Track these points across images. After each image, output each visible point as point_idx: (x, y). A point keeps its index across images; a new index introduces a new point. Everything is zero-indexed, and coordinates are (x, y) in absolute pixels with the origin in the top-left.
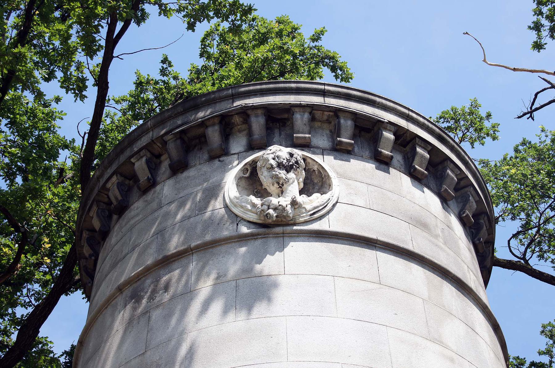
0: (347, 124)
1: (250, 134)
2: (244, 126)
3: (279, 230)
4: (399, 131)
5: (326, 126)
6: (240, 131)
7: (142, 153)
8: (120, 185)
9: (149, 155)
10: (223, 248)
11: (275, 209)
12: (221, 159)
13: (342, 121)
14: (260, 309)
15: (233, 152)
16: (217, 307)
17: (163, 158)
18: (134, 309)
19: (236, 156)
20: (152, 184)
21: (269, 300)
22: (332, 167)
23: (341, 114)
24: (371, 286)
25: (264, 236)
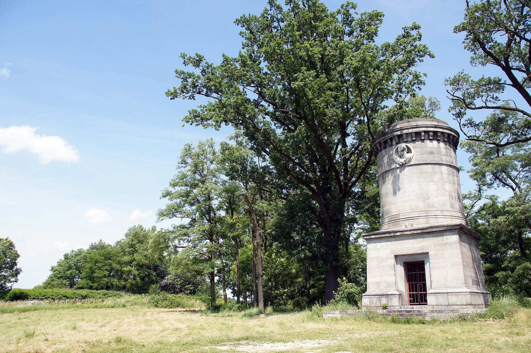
0: (414, 135)
4: (425, 132)
20: (381, 150)
22: (412, 146)
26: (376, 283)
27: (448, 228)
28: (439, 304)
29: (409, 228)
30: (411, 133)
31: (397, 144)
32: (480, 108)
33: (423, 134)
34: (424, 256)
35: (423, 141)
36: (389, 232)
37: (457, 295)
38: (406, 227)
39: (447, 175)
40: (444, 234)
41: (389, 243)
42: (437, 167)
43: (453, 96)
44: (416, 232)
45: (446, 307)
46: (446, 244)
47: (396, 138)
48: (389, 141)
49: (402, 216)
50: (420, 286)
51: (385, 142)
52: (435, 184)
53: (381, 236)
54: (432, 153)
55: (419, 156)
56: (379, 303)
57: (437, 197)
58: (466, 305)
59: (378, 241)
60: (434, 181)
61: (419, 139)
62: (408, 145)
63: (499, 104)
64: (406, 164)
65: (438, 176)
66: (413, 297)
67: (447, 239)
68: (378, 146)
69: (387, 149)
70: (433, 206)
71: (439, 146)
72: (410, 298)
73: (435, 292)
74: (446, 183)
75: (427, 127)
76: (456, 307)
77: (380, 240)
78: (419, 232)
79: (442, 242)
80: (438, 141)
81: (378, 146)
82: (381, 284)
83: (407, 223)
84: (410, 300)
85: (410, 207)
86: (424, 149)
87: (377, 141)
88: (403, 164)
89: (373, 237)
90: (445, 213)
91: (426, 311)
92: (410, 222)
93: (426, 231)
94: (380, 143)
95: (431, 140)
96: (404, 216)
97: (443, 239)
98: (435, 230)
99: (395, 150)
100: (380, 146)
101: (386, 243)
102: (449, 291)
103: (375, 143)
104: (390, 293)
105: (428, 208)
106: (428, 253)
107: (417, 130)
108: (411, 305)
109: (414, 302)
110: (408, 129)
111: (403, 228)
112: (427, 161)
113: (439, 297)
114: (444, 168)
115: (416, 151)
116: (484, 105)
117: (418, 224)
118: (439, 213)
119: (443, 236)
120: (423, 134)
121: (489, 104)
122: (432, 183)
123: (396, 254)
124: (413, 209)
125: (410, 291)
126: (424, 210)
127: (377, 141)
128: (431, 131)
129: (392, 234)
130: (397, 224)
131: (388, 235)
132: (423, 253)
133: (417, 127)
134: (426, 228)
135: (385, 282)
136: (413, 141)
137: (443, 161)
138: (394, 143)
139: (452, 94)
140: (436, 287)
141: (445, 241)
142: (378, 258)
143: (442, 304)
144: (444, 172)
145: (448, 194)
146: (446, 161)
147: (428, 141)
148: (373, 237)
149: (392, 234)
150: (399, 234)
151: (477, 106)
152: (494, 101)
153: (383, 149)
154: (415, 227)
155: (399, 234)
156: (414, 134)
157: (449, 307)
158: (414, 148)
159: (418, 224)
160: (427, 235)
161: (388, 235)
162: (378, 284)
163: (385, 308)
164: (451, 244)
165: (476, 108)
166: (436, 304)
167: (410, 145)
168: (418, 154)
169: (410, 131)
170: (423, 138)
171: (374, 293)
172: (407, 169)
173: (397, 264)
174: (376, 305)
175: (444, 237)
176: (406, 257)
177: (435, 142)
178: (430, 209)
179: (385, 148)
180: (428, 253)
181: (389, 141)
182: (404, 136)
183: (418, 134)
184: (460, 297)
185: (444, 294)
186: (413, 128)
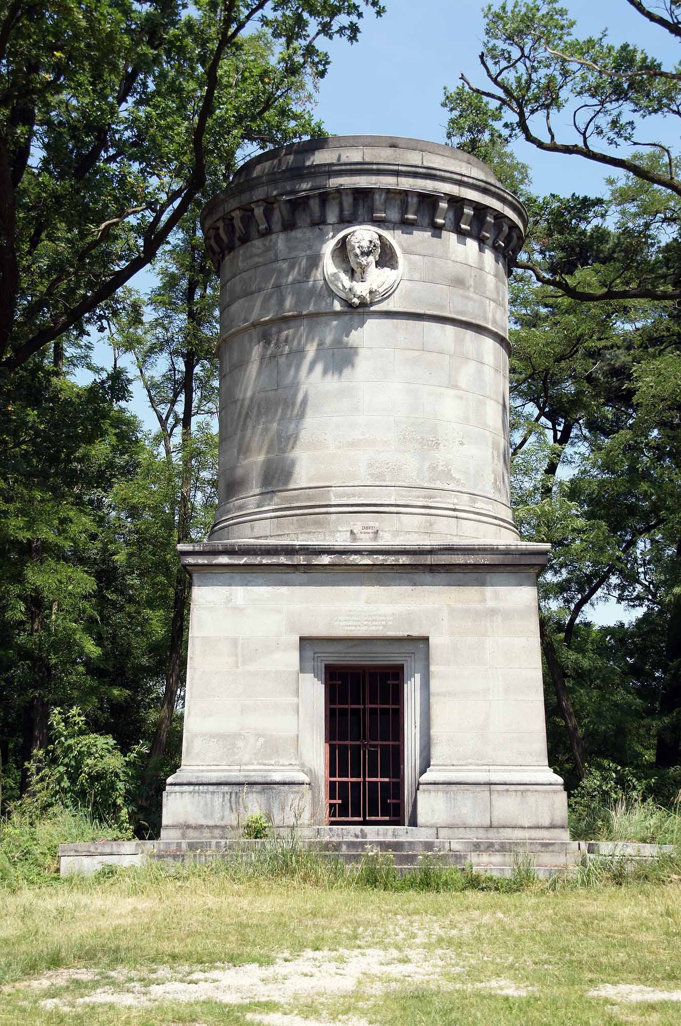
0: (413, 201)
1: (341, 210)
2: (337, 195)
3: (360, 310)
5: (398, 196)
6: (334, 199)
7: (260, 203)
8: (242, 218)
9: (265, 204)
10: (323, 319)
11: (359, 298)
12: (320, 227)
13: (410, 199)
14: (347, 372)
15: (329, 221)
16: (319, 368)
17: (275, 205)
18: (265, 348)
19: (331, 227)
20: (268, 232)
21: (353, 366)
22: (399, 243)
23: (410, 194)
24: (417, 353)
25: (351, 313)
26: (221, 737)
27: (508, 560)
28: (458, 821)
29: (365, 542)
30: (406, 192)
31: (345, 221)
32: (568, 150)
33: (444, 205)
34: (410, 648)
35: (437, 230)
36: (290, 551)
37: (522, 792)
38: (355, 540)
39: (492, 372)
40: (489, 577)
41: (284, 589)
42: (469, 334)
43: (495, 81)
44: (391, 560)
45: (481, 833)
46: (493, 612)
47: (348, 201)
48: (314, 204)
49: (337, 496)
50: (373, 755)
51: (299, 204)
52: (461, 398)
53: (257, 560)
54: (458, 282)
55: (419, 286)
56: (234, 816)
57: (462, 444)
58: (552, 827)
59: (237, 577)
60: (456, 387)
61: (426, 221)
62: (387, 234)
63: (624, 151)
64: (372, 304)
65: (471, 367)
66: (344, 797)
67: (497, 596)
68: (259, 212)
69: (297, 234)
70: (447, 475)
71: (481, 260)
72: (332, 796)
73: (447, 779)
74: (488, 401)
75: (460, 183)
76: (518, 834)
77: (249, 577)
78: (403, 560)
79: (479, 606)
80: (482, 241)
81: (259, 212)
82: (240, 743)
83: (358, 523)
84: (331, 806)
85: (370, 466)
86: (438, 261)
87: (260, 193)
88: (363, 304)
89: (224, 560)
90: (481, 505)
91: (456, 846)
92: (372, 521)
93: (429, 560)
94: (269, 204)
95: (462, 234)
96: (348, 496)
97: (483, 595)
98: (459, 559)
99: (334, 242)
100: (268, 214)
101: (270, 588)
102: (495, 778)
103: (245, 198)
104: (277, 777)
105: (431, 480)
106: (426, 639)
107: (428, 186)
108: (333, 823)
109: (343, 811)
110: (397, 174)
111: (341, 540)
112: (443, 307)
113: (459, 798)
114: (489, 344)
115: (412, 267)
116: (581, 144)
117: (396, 533)
118: (463, 502)
119: (483, 584)
120: (444, 205)
121: (597, 145)
122: (452, 392)
123: (306, 633)
124: (381, 476)
125: (332, 774)
126: (419, 483)
127: (260, 193)
128: (471, 202)
129: (301, 560)
130: (317, 523)
131: (283, 560)
132: (410, 639)
133: (430, 175)
134: (431, 552)
135: (259, 735)
136: (406, 225)
137: (486, 319)
138: (332, 217)
139: (494, 70)
140: (449, 762)
141: (491, 604)
142: (234, 642)
143: (471, 822)
144: (486, 361)
145: (490, 443)
146: (495, 322)
147: (453, 237)
148: (224, 560)
149: (301, 560)
150: (326, 560)
151: (559, 141)
152: (612, 135)
153: (276, 226)
154: (387, 540)
155: (326, 560)
156: (415, 200)
157: (492, 834)
158: (406, 252)
159: (396, 533)
160: (428, 577)
161: (283, 560)
162: (228, 740)
163: (257, 832)
164: (507, 615)
165: (554, 148)
166: (450, 821)
167: (394, 238)
168: (416, 276)
169: (406, 183)
170: (440, 221)
171: (214, 777)
172: (372, 324)
173: (302, 670)
174: (223, 823)
175: (489, 590)
176: (339, 647)
177: (472, 245)
178: (438, 485)
179: (289, 226)
180: (426, 639)
181: (314, 204)
182: (377, 197)
183: (428, 201)
184: (531, 799)
185: (478, 788)
186: (415, 175)
